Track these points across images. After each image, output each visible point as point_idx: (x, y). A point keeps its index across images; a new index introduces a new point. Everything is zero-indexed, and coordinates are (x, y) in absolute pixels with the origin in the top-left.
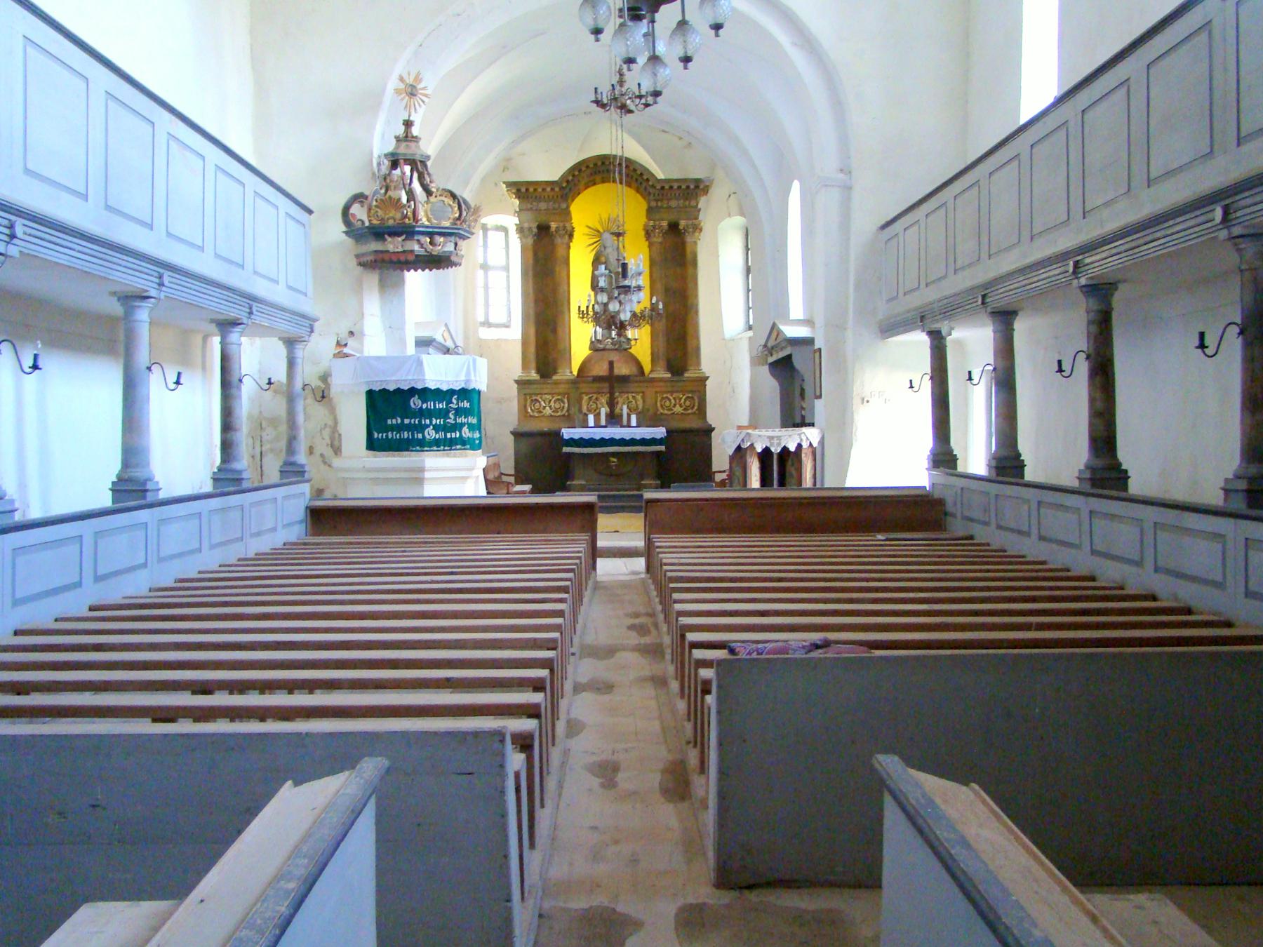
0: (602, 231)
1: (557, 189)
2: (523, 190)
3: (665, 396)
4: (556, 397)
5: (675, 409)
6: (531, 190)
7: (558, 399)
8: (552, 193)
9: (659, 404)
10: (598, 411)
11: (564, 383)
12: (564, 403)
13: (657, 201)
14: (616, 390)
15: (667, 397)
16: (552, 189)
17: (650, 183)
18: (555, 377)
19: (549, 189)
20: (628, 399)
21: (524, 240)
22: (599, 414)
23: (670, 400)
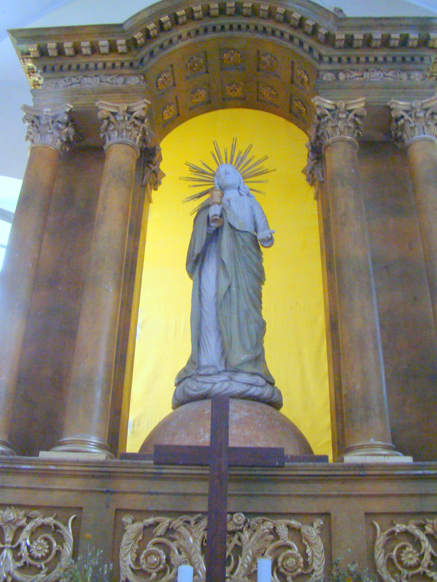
0: (214, 167)
1: (121, 42)
2: (52, 45)
3: (399, 527)
4: (39, 521)
6: (68, 45)
7: (44, 527)
8: (111, 59)
11: (74, 475)
12: (61, 539)
13: (336, 73)
14: (231, 505)
15: (406, 533)
16: (113, 48)
17: (322, 31)
18: (44, 455)
19: (103, 44)
20: (277, 537)
21: (38, 139)
23: (417, 544)
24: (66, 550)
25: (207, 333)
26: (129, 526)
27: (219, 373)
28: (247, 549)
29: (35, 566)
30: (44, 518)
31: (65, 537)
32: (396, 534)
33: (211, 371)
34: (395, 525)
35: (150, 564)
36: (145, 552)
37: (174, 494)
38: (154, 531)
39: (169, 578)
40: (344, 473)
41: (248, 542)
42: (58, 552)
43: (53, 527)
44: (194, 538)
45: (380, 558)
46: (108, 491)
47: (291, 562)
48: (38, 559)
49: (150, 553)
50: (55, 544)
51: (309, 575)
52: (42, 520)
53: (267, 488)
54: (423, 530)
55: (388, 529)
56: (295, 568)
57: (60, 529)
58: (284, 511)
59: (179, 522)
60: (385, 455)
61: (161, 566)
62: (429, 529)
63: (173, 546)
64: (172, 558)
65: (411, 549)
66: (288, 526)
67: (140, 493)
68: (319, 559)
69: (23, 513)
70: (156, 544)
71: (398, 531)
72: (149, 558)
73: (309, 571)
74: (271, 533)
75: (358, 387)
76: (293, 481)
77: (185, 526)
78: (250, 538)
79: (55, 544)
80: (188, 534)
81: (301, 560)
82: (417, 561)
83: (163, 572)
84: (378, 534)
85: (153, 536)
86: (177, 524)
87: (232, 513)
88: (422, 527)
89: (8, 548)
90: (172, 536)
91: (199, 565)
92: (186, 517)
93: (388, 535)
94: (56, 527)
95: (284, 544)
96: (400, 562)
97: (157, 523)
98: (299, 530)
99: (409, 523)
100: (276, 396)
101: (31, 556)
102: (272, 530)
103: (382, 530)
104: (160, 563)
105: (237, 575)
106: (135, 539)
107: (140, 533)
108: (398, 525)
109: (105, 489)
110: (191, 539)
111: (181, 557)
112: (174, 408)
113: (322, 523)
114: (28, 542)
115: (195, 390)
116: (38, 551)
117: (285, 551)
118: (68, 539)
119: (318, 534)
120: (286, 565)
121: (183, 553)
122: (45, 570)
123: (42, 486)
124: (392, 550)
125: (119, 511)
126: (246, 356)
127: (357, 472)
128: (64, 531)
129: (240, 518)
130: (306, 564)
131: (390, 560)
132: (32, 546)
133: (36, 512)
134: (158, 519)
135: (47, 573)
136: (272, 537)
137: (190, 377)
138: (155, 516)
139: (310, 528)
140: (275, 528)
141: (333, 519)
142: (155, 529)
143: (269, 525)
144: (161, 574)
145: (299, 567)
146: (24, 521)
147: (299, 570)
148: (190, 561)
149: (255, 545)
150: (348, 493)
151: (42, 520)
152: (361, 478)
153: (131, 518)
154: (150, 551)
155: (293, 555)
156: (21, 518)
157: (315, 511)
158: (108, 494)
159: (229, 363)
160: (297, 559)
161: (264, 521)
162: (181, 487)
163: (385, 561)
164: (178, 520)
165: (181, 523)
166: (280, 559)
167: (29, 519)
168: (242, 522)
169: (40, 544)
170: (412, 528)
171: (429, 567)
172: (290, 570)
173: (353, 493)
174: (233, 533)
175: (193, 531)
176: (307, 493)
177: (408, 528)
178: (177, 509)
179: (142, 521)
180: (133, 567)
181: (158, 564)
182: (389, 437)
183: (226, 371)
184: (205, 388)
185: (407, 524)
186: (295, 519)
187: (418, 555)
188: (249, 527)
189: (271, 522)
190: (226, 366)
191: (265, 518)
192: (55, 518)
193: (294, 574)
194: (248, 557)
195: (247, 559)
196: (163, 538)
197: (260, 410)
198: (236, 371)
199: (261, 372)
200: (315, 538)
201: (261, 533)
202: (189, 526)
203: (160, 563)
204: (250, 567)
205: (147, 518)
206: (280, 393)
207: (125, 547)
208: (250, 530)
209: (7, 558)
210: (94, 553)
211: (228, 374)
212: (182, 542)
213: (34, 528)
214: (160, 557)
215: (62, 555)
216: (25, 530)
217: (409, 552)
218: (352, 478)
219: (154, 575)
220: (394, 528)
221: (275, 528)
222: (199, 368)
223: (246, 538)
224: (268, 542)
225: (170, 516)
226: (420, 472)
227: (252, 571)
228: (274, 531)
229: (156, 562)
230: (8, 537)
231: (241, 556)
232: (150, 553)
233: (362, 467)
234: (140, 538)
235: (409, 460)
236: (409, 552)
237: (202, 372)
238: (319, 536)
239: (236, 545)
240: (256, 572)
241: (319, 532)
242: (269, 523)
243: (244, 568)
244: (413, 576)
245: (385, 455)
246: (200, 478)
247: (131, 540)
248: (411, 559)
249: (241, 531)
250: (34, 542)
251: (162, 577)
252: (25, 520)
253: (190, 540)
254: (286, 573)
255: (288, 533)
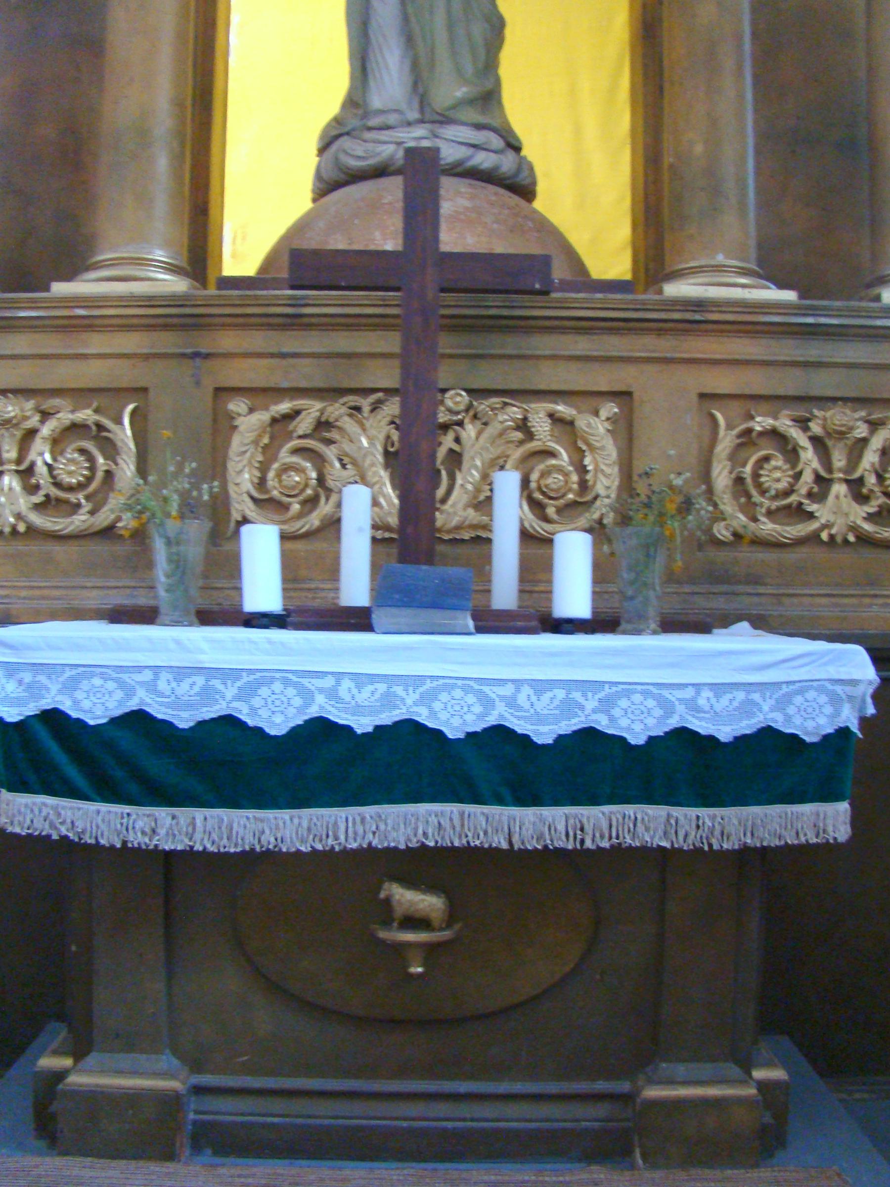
3: (761, 423)
4: (66, 417)
5: (823, 512)
7: (76, 428)
9: (722, 478)
10: (325, 508)
11: (126, 326)
12: (110, 448)
14: (444, 375)
15: (774, 434)
18: (60, 288)
20: (530, 435)
22: (333, 524)
23: (792, 453)
24: (122, 469)
25: (381, 39)
26: (242, 419)
27: (409, 124)
28: (473, 458)
29: (67, 502)
30: (73, 412)
31: (119, 444)
32: (754, 434)
33: (392, 119)
34: (752, 418)
35: (285, 487)
36: (276, 466)
37: (328, 356)
38: (291, 427)
39: (324, 512)
40: (663, 315)
41: (473, 445)
42: (109, 474)
43: (94, 428)
44: (371, 439)
45: (721, 478)
46: (196, 355)
47: (554, 481)
48: (71, 489)
49: (286, 468)
50: (101, 460)
51: (589, 504)
52: (71, 416)
53: (511, 344)
54: (806, 429)
55: (741, 424)
56: (563, 491)
57: (109, 431)
58: (542, 387)
59: (340, 408)
60: (744, 286)
61: (309, 492)
62: (816, 428)
63: (330, 452)
64: (328, 477)
65: (780, 463)
66: (551, 416)
67: (260, 355)
68: (607, 476)
69: (30, 404)
70: (297, 451)
71: (758, 428)
72: (284, 477)
73: (588, 498)
74: (518, 428)
75: (699, 149)
76: (563, 330)
77: (351, 415)
78: (477, 438)
79: (101, 460)
80: (359, 431)
81: (575, 478)
82: (789, 483)
83: (311, 503)
84: (722, 432)
85: (289, 436)
86: (337, 413)
87: (444, 391)
88: (803, 423)
89: (9, 471)
90: (327, 435)
91: (381, 488)
92: (352, 399)
93: (739, 436)
94: (100, 427)
95: (543, 448)
96: (758, 485)
97: (297, 413)
98: (572, 423)
99: (779, 416)
100: (525, 173)
101: (58, 485)
102: (520, 423)
103: (730, 427)
104: (306, 486)
105: (453, 506)
106: (256, 442)
107: (264, 432)
108: (758, 419)
109: (189, 351)
110: (365, 442)
111: (345, 473)
112: (314, 200)
113: (616, 410)
114: (49, 461)
115: (359, 158)
116: (70, 473)
117: (543, 462)
118: (125, 449)
119: (608, 431)
120: (546, 486)
121: (348, 466)
122: (87, 506)
123: (60, 351)
124: (744, 465)
125: (222, 392)
126: (464, 89)
127: (688, 316)
128: (116, 434)
129: (458, 399)
130: (584, 486)
131: (739, 480)
132: (56, 465)
133: (56, 402)
134: (299, 403)
135: (92, 513)
136: (519, 435)
137: (348, 134)
138: (292, 399)
139: (593, 420)
140: (525, 419)
141: (636, 404)
142: (294, 423)
143: (515, 412)
144: (308, 506)
145: (570, 490)
146: (34, 421)
147: (571, 496)
148: (363, 479)
149: (487, 449)
150: (668, 355)
151: (71, 416)
152: (695, 326)
153: (246, 404)
154: (285, 464)
155: (560, 469)
156: (28, 414)
157: (604, 388)
158: (198, 360)
159: (429, 104)
160: (566, 475)
161: (506, 404)
162: (343, 342)
163: (730, 483)
164: (337, 405)
165: (344, 410)
166: (534, 476)
167: (46, 415)
168: (462, 407)
169: (72, 461)
170: (785, 424)
171: (810, 495)
172: (552, 494)
173: (677, 355)
174: (445, 427)
175: (367, 424)
176: (588, 353)
177: (777, 424)
178: (336, 385)
179: (266, 409)
180: (256, 495)
181: (301, 487)
182: (753, 253)
183: (422, 121)
184: (379, 154)
185: (776, 418)
186: (566, 404)
187: (791, 473)
188: (475, 417)
189: (518, 407)
190: (422, 110)
191: (507, 400)
192: (96, 411)
193: (562, 502)
194: (474, 472)
195: (472, 476)
196: (311, 439)
197: (494, 198)
198: (445, 120)
199: (495, 123)
200: (602, 438)
201: (500, 427)
202: (360, 416)
203: (306, 486)
204: (478, 490)
205: (276, 403)
206: (531, 168)
207: (238, 459)
208: (478, 423)
209: (11, 489)
210: (180, 466)
211: (427, 125)
212: (347, 447)
213: (58, 430)
214: (306, 474)
215: (116, 479)
216: (39, 436)
217: (776, 468)
218: (680, 326)
219: (296, 507)
220: (750, 424)
221: (525, 419)
222: (366, 115)
223: (470, 437)
224: (510, 445)
225: (322, 399)
226: (810, 320)
227: (482, 497)
228: (523, 426)
229: (298, 483)
230: (8, 451)
231: (460, 470)
232: (286, 468)
233: (699, 305)
234: (266, 440)
235: (789, 296)
236: (776, 468)
237: (374, 122)
238: (609, 434)
239: (451, 451)
240: (489, 499)
241: (610, 428)
242: (515, 409)
243: (466, 493)
244: (779, 509)
245: (744, 286)
246: (380, 323)
247: (248, 444)
248: (778, 480)
249: (460, 424)
250: (60, 458)
251: (311, 511)
252: (37, 417)
253: (360, 441)
254: (546, 501)
255: (552, 430)
